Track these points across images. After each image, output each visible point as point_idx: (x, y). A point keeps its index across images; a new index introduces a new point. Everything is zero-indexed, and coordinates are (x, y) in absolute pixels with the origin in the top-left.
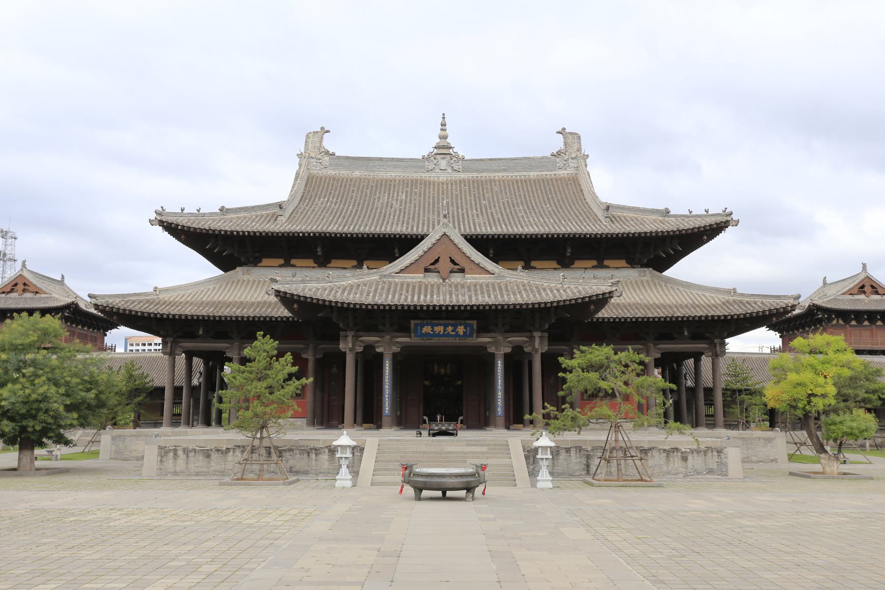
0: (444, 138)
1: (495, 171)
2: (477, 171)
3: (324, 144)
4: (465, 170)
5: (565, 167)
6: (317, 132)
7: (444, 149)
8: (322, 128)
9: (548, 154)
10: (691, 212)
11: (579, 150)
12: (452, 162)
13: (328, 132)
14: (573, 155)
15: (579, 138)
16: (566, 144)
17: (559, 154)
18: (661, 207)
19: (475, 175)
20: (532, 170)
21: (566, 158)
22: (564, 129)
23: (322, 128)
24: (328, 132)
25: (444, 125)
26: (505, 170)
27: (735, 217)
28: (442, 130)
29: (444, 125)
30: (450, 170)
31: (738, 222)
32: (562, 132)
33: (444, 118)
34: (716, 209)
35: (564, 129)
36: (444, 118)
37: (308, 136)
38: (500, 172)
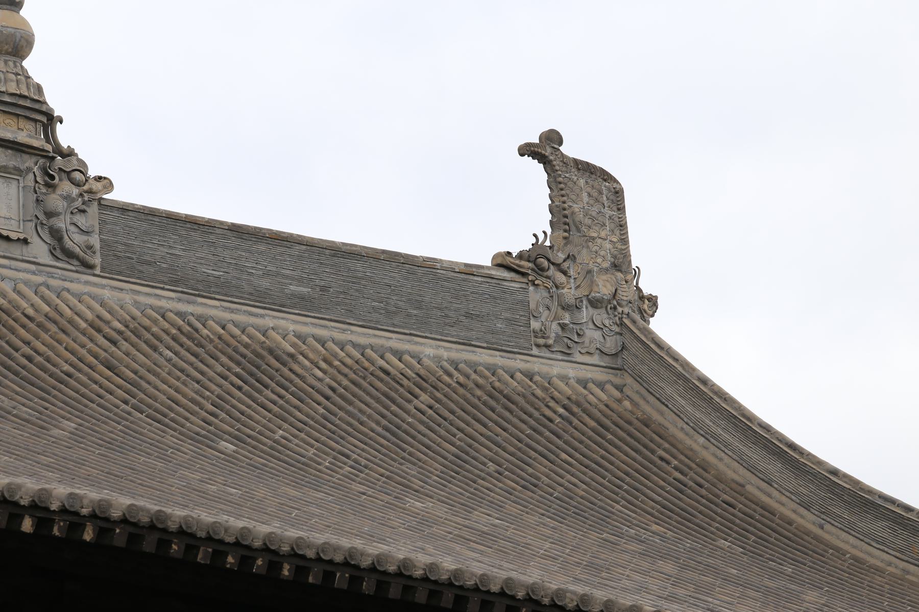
1: (262, 299)
2: (177, 281)
4: (123, 265)
5: (567, 343)
11: (621, 263)
12: (55, 201)
14: (604, 289)
15: (618, 194)
16: (560, 216)
17: (526, 267)
19: (168, 300)
21: (569, 293)
22: (553, 138)
26: (303, 305)
30: (39, 250)
32: (545, 150)
35: (553, 138)
38: (280, 306)
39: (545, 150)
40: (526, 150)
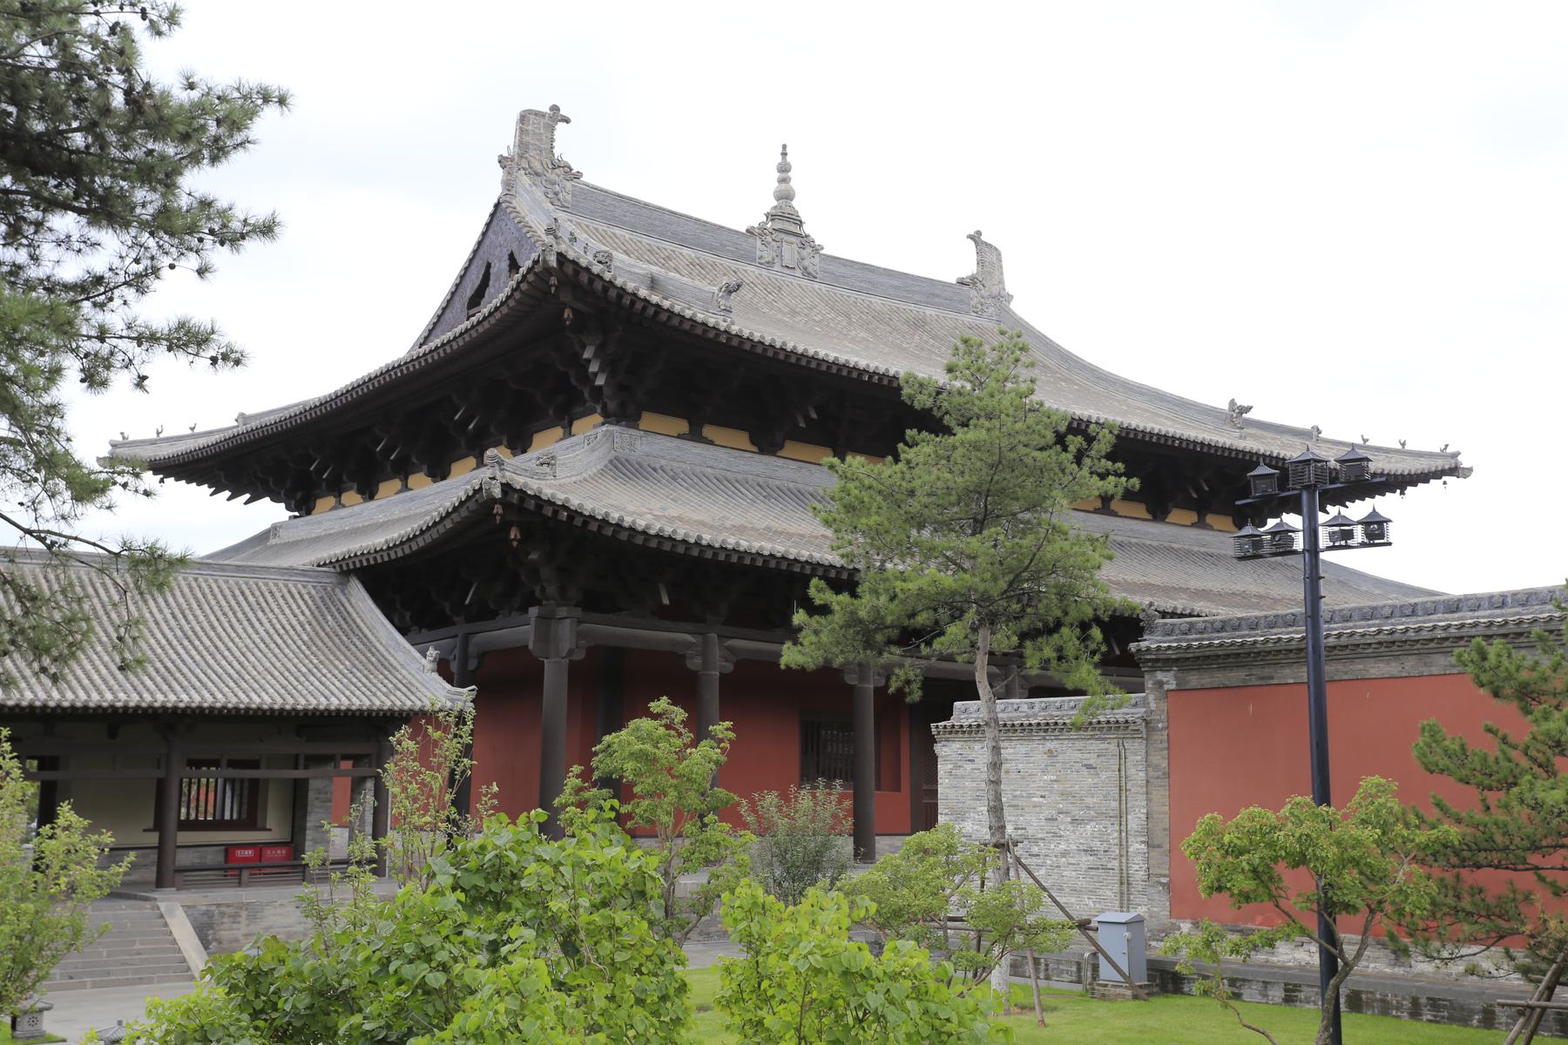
0: (785, 196)
3: (557, 152)
6: (543, 115)
7: (785, 219)
8: (555, 108)
9: (952, 279)
10: (1365, 441)
11: (1001, 282)
12: (804, 253)
13: (567, 121)
16: (980, 263)
18: (1305, 424)
20: (928, 304)
22: (979, 233)
23: (555, 108)
24: (567, 121)
25: (784, 169)
27: (1465, 462)
28: (784, 181)
29: (784, 169)
30: (798, 273)
31: (1470, 470)
32: (976, 238)
33: (784, 154)
34: (1426, 441)
35: (979, 233)
36: (784, 154)
37: (524, 117)
39: (976, 238)
40: (970, 237)
